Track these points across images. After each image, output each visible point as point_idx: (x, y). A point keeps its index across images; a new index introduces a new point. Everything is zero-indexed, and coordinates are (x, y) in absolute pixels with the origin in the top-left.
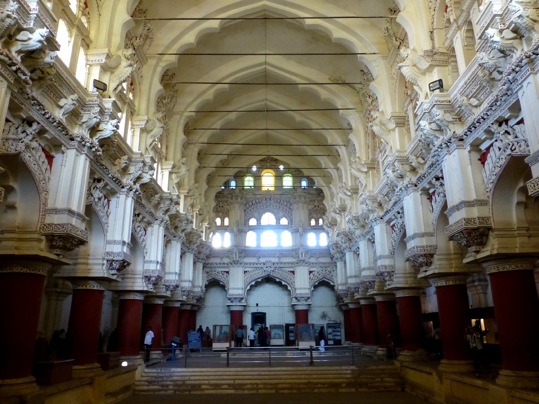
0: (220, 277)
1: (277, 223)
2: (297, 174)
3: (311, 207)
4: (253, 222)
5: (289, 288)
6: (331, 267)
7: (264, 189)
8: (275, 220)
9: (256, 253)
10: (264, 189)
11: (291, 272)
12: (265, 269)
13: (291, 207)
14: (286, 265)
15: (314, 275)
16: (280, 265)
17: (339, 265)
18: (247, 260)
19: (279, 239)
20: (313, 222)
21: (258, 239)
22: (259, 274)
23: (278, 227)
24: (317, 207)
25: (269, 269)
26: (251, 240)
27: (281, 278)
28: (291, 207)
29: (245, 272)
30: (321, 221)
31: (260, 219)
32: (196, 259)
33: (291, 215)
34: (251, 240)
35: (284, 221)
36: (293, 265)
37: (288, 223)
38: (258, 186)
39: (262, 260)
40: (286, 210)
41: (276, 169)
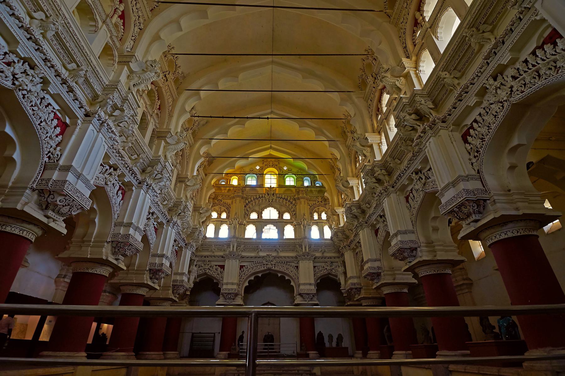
0: (213, 273)
1: (279, 217)
2: (300, 175)
4: (254, 216)
7: (267, 185)
8: (278, 215)
10: (267, 185)
17: (348, 256)
20: (316, 217)
21: (259, 231)
26: (250, 232)
31: (261, 213)
32: (182, 244)
34: (250, 232)
35: (287, 216)
38: (261, 185)
41: (280, 169)
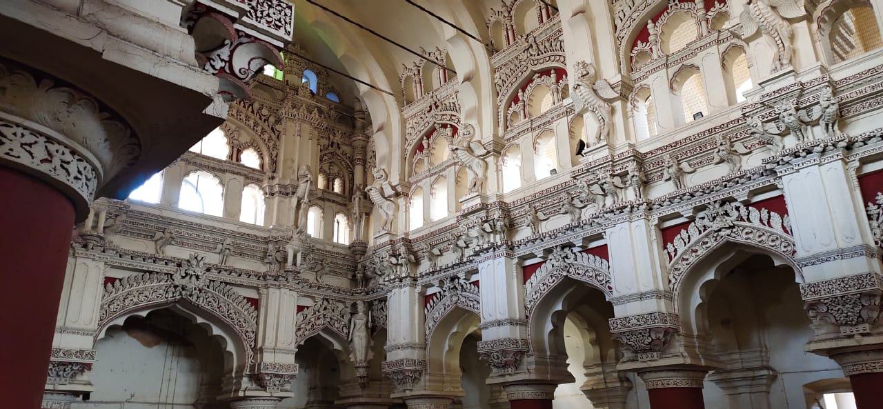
1: (231, 156)
3: (325, 142)
5: (230, 347)
6: (349, 303)
9: (162, 226)
11: (249, 300)
12: (178, 280)
13: (278, 127)
14: (244, 280)
15: (305, 318)
16: (224, 276)
18: (118, 241)
19: (232, 202)
22: (153, 293)
23: (226, 170)
24: (335, 145)
25: (193, 284)
27: (218, 313)
28: (278, 127)
29: (109, 281)
30: (337, 188)
33: (275, 146)
35: (250, 159)
36: (261, 283)
37: (262, 166)
39: (172, 251)
40: (263, 131)
